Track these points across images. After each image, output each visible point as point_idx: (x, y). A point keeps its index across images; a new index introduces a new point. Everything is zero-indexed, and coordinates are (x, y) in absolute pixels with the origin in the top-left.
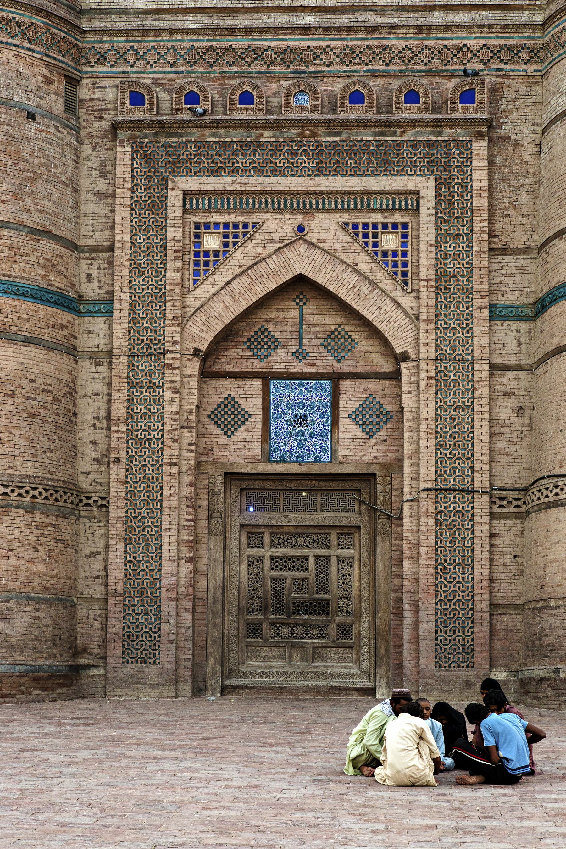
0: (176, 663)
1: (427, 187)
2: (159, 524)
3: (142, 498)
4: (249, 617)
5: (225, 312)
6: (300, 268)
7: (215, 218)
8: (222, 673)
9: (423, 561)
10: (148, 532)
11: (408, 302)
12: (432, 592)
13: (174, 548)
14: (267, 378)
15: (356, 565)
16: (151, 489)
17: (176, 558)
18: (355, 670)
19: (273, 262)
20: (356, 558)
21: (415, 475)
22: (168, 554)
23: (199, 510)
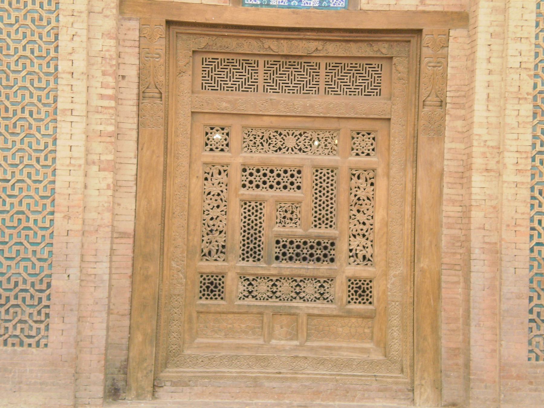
0: (77, 343)
2: (51, 100)
3: (21, 52)
4: (204, 263)
8: (156, 359)
9: (510, 176)
10: (31, 113)
12: (525, 230)
13: (79, 140)
15: (381, 183)
16: (36, 38)
17: (82, 162)
18: (377, 356)
20: (380, 171)
21: (498, 29)
22: (69, 154)
23: (123, 84)
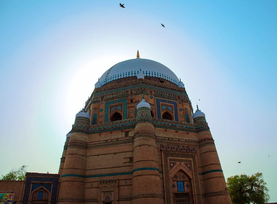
1: (192, 160)
5: (174, 173)
6: (181, 168)
7: (172, 162)
11: (191, 172)
14: (177, 181)
19: (178, 167)
